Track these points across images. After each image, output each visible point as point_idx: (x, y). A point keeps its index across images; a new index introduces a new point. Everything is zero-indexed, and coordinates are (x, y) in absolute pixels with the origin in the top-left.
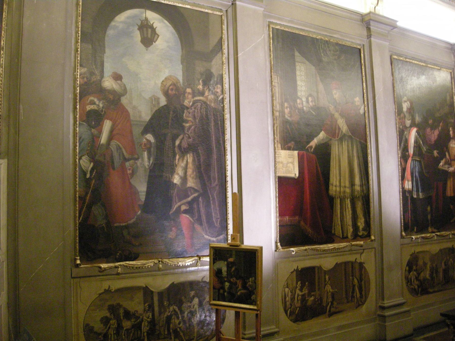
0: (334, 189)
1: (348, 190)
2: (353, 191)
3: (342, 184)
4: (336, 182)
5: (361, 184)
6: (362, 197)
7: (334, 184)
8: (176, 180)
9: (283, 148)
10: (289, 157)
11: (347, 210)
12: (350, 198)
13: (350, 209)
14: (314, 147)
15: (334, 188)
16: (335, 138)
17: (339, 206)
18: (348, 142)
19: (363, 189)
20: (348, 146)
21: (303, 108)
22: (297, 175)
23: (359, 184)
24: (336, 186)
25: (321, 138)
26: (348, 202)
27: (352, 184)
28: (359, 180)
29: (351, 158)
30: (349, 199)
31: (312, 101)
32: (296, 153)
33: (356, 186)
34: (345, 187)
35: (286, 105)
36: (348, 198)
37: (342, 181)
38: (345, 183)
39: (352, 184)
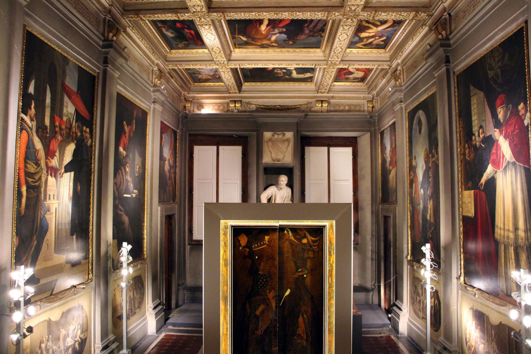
0: (499, 232)
1: (512, 236)
2: (516, 237)
3: (506, 227)
4: (501, 223)
5: (526, 229)
6: (527, 248)
7: (499, 226)
8: (428, 218)
9: (466, 190)
10: (469, 197)
11: (511, 261)
12: (514, 245)
13: (513, 261)
14: (483, 184)
15: (499, 231)
16: (499, 170)
17: (503, 254)
18: (511, 170)
19: (528, 237)
20: (512, 176)
21: (476, 144)
22: (473, 215)
23: (523, 228)
24: (500, 229)
25: (489, 173)
26: (512, 250)
27: (516, 229)
28: (523, 222)
29: (515, 192)
30: (512, 247)
31: (482, 134)
32: (472, 191)
33: (519, 231)
34: (509, 230)
35: (467, 146)
36: (511, 246)
37: (506, 222)
38: (509, 226)
39: (516, 229)
